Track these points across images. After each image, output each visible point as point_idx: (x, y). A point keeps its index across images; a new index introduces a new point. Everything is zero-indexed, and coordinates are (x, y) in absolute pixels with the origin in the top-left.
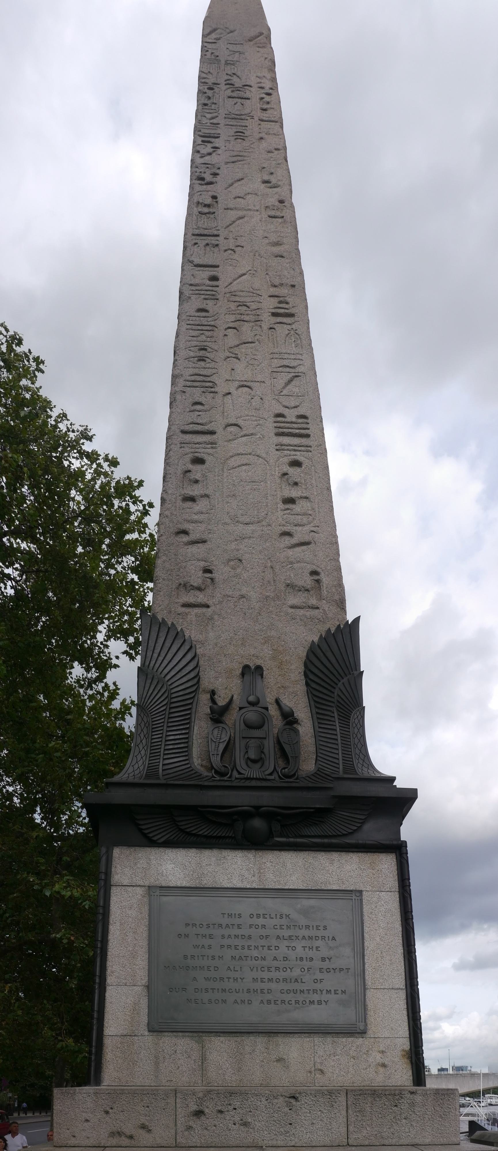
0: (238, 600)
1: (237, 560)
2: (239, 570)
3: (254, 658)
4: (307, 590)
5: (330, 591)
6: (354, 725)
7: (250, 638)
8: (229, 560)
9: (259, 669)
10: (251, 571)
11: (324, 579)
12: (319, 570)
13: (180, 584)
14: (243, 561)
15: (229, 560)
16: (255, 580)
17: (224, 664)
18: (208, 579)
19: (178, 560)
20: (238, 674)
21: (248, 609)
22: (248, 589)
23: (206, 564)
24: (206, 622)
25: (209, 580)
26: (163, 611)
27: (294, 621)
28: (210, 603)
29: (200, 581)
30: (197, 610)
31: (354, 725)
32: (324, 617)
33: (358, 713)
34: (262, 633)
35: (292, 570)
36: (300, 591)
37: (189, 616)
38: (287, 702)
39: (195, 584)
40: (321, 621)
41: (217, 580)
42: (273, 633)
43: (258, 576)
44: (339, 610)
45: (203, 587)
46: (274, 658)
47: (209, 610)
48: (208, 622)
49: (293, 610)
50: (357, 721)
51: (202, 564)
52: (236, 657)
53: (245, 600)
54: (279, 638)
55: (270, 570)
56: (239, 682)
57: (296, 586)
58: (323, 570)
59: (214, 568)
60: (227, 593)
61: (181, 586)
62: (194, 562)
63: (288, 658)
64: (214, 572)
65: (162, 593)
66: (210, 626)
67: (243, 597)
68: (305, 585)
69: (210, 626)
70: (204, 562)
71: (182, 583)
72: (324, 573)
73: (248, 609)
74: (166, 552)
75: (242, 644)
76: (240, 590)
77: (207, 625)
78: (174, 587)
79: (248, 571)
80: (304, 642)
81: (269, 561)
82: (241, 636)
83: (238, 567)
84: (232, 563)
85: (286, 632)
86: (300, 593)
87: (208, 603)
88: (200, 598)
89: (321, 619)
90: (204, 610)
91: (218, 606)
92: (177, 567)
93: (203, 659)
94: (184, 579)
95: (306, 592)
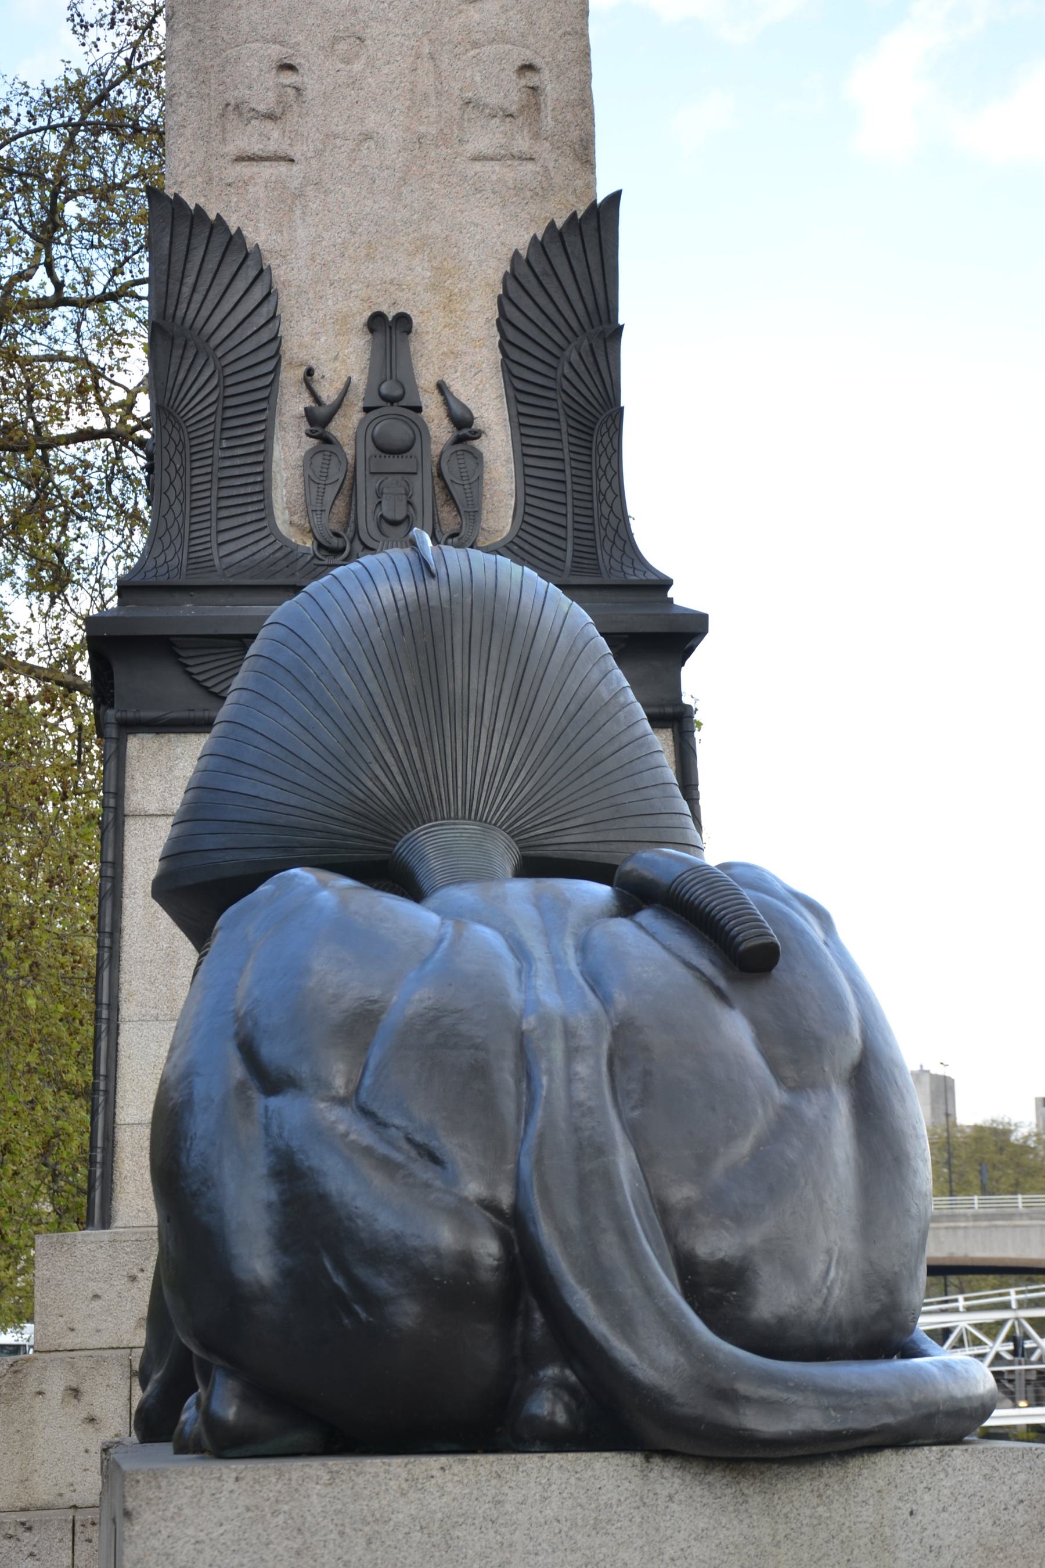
0: (358, 145)
1: (353, 39)
2: (357, 67)
3: (392, 289)
4: (511, 115)
5: (560, 118)
6: (601, 449)
7: (384, 242)
8: (336, 40)
9: (404, 321)
10: (386, 70)
11: (549, 88)
12: (538, 62)
13: (228, 105)
14: (369, 42)
15: (336, 40)
16: (395, 93)
17: (330, 303)
18: (289, 90)
19: (219, 41)
20: (360, 326)
21: (380, 168)
22: (378, 119)
23: (284, 50)
24: (289, 202)
25: (291, 92)
26: (194, 177)
27: (478, 196)
28: (296, 153)
29: (271, 96)
30: (267, 170)
31: (601, 449)
32: (545, 185)
33: (610, 422)
34: (410, 230)
35: (478, 65)
36: (495, 116)
37: (251, 189)
38: (462, 391)
39: (262, 108)
40: (537, 194)
41: (309, 94)
42: (435, 228)
43: (401, 82)
44: (578, 165)
45: (278, 111)
46: (434, 287)
47: (295, 168)
48: (293, 203)
49: (478, 166)
50: (606, 439)
51: (275, 52)
52: (354, 287)
53: (371, 144)
54: (446, 239)
55: (428, 65)
56: (362, 342)
57: (486, 106)
58: (547, 63)
59: (303, 61)
60: (334, 128)
61: (230, 108)
62: (254, 46)
63: (463, 285)
64: (301, 71)
65: (188, 132)
66: (298, 213)
67: (367, 137)
68: (506, 105)
69: (298, 213)
70: (278, 47)
71: (233, 103)
72: (551, 71)
73: (380, 168)
74: (191, 21)
75: (367, 255)
76: (362, 120)
77: (291, 210)
78: (215, 114)
79: (379, 69)
80: (498, 247)
81: (425, 41)
82: (364, 238)
83: (357, 56)
84: (342, 46)
85: (460, 223)
86: (496, 121)
87: (291, 154)
88: (274, 138)
89: (539, 190)
90: (283, 168)
91: (313, 161)
92: (218, 61)
93: (286, 293)
94: (236, 93)
95: (508, 120)
